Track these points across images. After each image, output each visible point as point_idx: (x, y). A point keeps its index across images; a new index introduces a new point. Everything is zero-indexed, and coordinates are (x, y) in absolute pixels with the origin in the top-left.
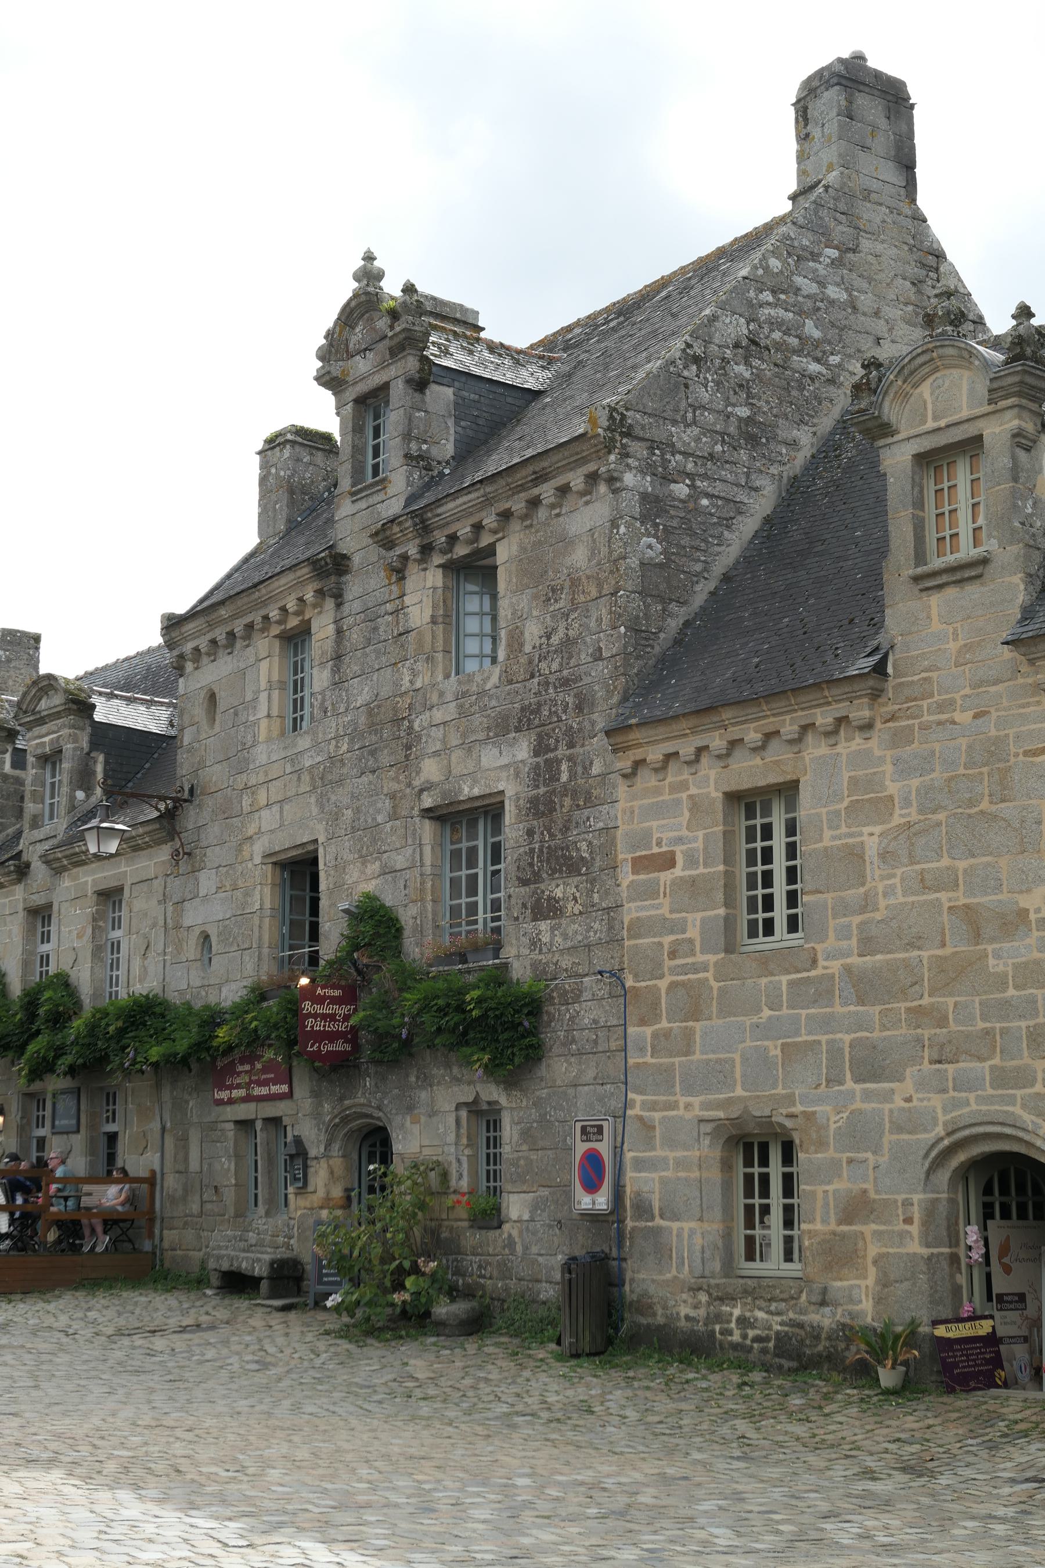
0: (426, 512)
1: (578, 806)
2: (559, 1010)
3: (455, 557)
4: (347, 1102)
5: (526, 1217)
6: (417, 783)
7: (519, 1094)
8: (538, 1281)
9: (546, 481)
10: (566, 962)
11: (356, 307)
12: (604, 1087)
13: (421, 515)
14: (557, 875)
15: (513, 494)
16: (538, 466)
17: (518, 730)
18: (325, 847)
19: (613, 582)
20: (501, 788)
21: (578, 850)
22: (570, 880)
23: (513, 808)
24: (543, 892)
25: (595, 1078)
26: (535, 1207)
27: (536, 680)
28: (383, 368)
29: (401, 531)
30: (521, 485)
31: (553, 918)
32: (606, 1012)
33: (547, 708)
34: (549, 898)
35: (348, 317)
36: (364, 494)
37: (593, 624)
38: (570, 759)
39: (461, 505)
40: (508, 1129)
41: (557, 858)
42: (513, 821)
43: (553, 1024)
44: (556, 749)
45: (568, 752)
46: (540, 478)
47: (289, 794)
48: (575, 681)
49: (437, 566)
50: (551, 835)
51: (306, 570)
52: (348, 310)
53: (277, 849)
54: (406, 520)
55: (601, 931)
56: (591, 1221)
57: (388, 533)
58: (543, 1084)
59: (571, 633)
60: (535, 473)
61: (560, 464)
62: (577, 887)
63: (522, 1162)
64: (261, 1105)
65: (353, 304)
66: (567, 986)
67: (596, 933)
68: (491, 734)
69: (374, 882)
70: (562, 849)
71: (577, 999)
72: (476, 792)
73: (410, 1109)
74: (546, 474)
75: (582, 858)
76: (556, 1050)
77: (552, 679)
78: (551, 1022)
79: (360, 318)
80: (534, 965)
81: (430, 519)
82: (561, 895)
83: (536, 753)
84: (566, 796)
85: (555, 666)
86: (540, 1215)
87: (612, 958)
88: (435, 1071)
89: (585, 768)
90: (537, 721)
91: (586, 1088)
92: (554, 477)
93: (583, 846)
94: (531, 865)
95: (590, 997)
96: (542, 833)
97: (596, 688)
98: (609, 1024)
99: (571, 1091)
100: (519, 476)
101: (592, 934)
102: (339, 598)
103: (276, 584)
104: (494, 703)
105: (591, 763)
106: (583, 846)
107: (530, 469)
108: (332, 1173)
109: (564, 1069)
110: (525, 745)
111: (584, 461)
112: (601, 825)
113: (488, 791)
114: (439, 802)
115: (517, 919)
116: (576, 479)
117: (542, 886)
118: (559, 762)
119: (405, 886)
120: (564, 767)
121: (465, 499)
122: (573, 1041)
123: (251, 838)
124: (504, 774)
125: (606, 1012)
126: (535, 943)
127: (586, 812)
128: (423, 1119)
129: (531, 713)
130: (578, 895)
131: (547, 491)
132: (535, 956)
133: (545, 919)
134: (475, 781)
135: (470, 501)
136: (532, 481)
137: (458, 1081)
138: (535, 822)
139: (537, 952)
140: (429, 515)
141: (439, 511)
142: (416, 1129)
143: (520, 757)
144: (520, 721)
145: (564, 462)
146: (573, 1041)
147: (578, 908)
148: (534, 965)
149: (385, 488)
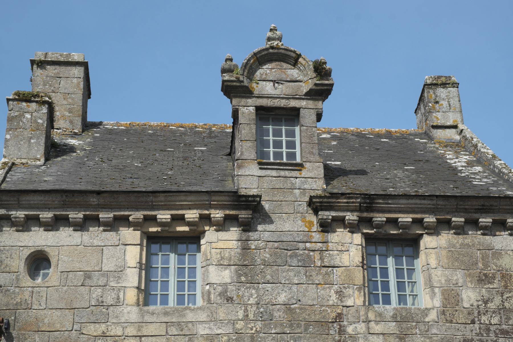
3: (383, 232)
15: (456, 211)
30: (465, 209)
36: (276, 167)
49: (363, 234)
51: (227, 198)
59: (507, 304)
60: (483, 205)
61: (505, 207)
85: (495, 320)
100: (469, 203)
135: (420, 204)
136: (475, 209)
145: (509, 207)
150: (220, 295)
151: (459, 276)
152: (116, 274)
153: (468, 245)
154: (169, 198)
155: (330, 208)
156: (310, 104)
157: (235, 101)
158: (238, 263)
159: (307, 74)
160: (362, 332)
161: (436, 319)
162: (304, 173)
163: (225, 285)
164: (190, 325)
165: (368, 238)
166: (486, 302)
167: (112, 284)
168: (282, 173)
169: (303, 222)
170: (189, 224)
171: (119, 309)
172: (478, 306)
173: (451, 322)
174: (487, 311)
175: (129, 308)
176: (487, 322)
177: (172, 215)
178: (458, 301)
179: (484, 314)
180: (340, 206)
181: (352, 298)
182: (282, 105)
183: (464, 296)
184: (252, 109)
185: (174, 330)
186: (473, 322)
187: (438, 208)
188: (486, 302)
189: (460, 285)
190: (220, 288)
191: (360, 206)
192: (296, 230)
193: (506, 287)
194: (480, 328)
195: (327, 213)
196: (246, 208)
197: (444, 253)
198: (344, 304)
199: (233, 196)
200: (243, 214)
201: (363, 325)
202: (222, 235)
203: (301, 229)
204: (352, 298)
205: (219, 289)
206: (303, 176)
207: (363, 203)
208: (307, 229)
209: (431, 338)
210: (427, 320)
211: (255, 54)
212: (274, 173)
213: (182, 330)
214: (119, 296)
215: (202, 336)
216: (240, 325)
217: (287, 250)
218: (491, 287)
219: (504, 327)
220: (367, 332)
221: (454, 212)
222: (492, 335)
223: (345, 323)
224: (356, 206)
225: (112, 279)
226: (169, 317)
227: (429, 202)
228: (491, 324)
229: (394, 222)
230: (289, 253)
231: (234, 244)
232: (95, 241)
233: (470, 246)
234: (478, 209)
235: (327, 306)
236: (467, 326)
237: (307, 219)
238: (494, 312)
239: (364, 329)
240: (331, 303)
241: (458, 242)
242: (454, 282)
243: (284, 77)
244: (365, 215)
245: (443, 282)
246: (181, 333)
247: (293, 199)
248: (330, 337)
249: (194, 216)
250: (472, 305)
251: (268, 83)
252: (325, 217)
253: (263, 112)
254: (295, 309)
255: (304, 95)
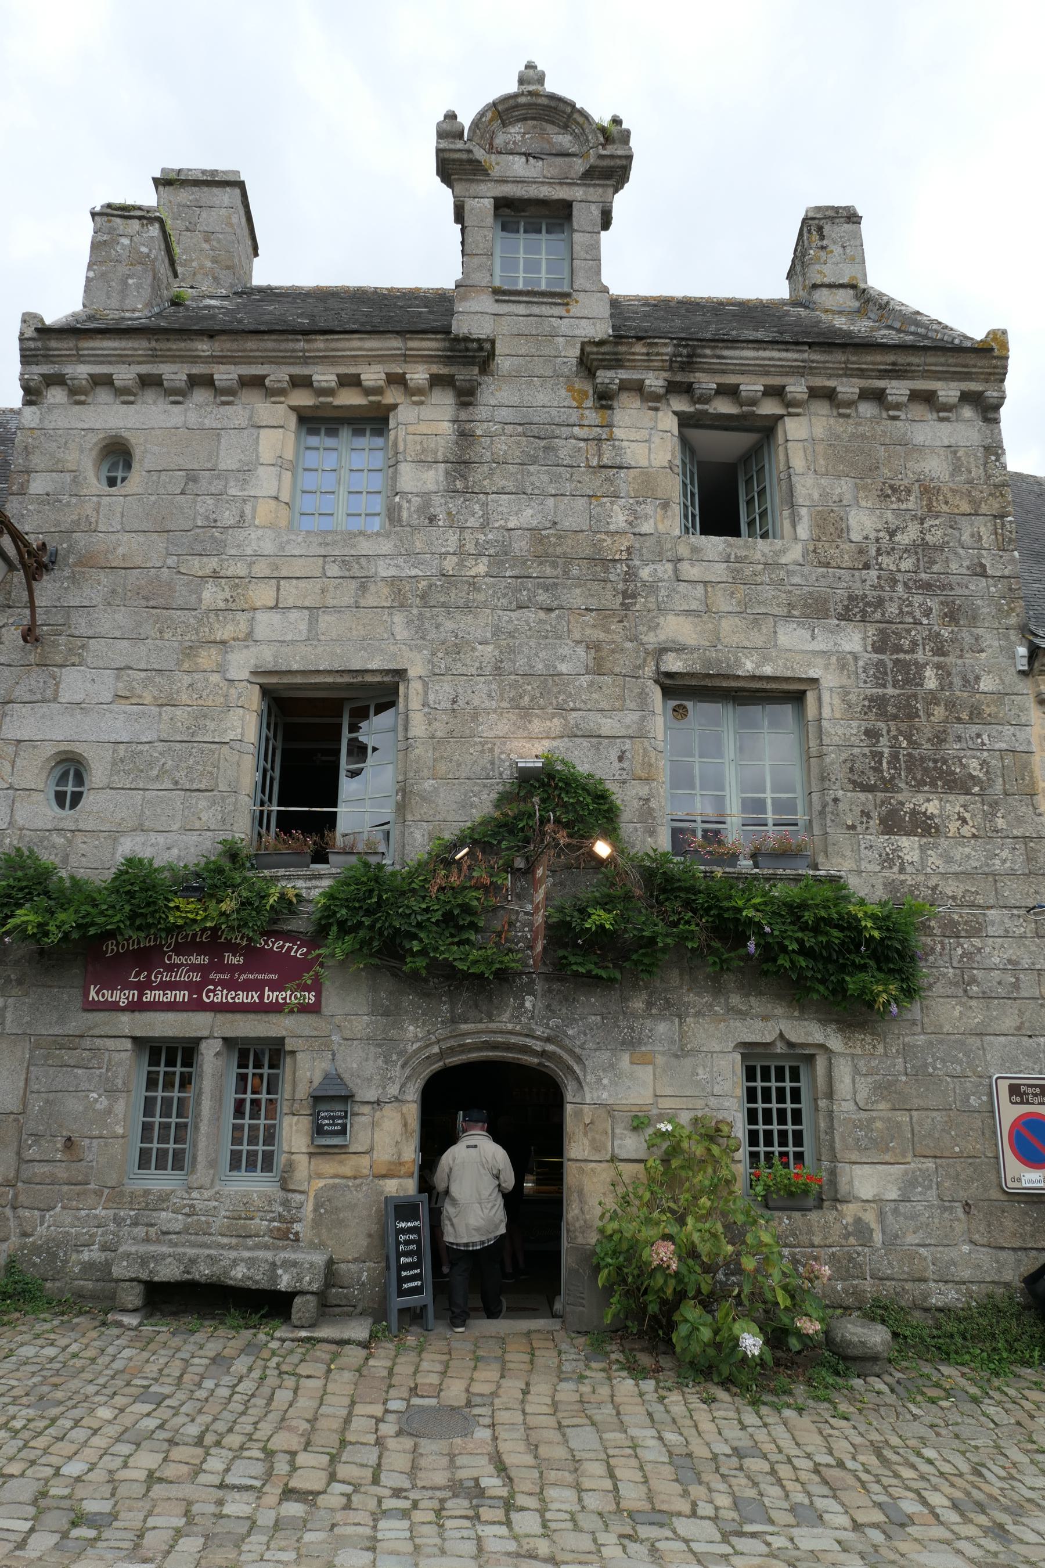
0: (704, 347)
1: (959, 720)
2: (942, 943)
3: (711, 411)
4: (464, 1027)
5: (893, 1194)
6: (652, 640)
7: (869, 1038)
8: (925, 1280)
9: (905, 378)
10: (951, 888)
11: (524, 105)
12: (1035, 1039)
13: (694, 347)
14: (926, 788)
15: (846, 375)
16: (902, 359)
17: (841, 617)
18: (425, 685)
19: (997, 506)
20: (812, 674)
21: (964, 766)
22: (951, 797)
23: (836, 701)
24: (902, 804)
25: (1018, 1028)
26: (909, 1183)
27: (873, 573)
28: (561, 184)
29: (648, 354)
31: (922, 836)
32: (1031, 953)
33: (895, 605)
34: (914, 812)
35: (507, 110)
37: (966, 537)
38: (938, 666)
39: (764, 359)
40: (848, 1080)
41: (926, 770)
42: (838, 715)
43: (931, 958)
44: (912, 651)
45: (936, 659)
46: (896, 373)
47: (331, 602)
48: (943, 587)
49: (675, 413)
50: (911, 742)
52: (511, 102)
53: (295, 667)
54: (665, 344)
55: (1013, 862)
56: (1025, 1203)
57: (622, 349)
58: (919, 1029)
59: (928, 537)
60: (894, 364)
61: (933, 368)
62: (964, 806)
63: (879, 1124)
64: (220, 1017)
65: (522, 100)
66: (956, 917)
67: (1004, 861)
68: (795, 613)
69: (546, 743)
70: (935, 761)
71: (976, 930)
72: (768, 670)
73: (630, 1044)
74: (906, 371)
75: (973, 777)
76: (938, 989)
77: (899, 577)
78: (927, 955)
79: (518, 121)
80: (891, 886)
81: (705, 356)
82: (936, 812)
83: (877, 649)
84: (937, 704)
85: (906, 565)
86: (921, 1193)
87: (1036, 892)
88: (691, 998)
89: (966, 681)
90: (878, 616)
91: (1002, 1039)
92: (912, 378)
93: (974, 764)
94: (877, 769)
95: (1001, 933)
96: (896, 738)
97: (979, 602)
98: (1038, 967)
99: (974, 1041)
100: (869, 358)
101: (997, 862)
102: (466, 396)
103: (356, 344)
104: (796, 580)
105: (978, 678)
106: (974, 764)
107: (891, 358)
108: (405, 1125)
109: (957, 1013)
110: (857, 637)
111: (967, 377)
112: (1004, 746)
113: (789, 674)
114: (698, 668)
115: (853, 827)
116: (948, 392)
117: (900, 797)
118: (921, 667)
119: (621, 759)
120: (929, 672)
121: (776, 354)
122: (973, 980)
123: (223, 642)
124: (820, 661)
125: (1031, 953)
126: (888, 860)
127: (975, 729)
128: (660, 1060)
129: (868, 604)
130: (967, 815)
131: (898, 389)
132: (893, 873)
133: (908, 835)
134: (765, 659)
135: (780, 359)
136: (880, 371)
137: (742, 1015)
138: (881, 725)
139: (896, 869)
140: (708, 352)
141: (726, 353)
142: (645, 1073)
143: (847, 647)
144: (847, 608)
145: (940, 368)
146: (973, 980)
147: (966, 831)
148: (891, 886)
149: (567, 304)
150: (417, 511)
151: (844, 488)
152: (240, 476)
153: (863, 436)
154: (333, 345)
155: (616, 363)
156: (594, 193)
157: (458, 187)
158: (452, 459)
159: (587, 140)
160: (666, 577)
161: (801, 561)
162: (574, 310)
163: (425, 495)
164: (363, 561)
165: (685, 421)
166: (892, 534)
167: (232, 491)
168: (535, 310)
169: (569, 391)
170: (368, 392)
171: (241, 534)
172: (877, 540)
173: (827, 565)
174: (893, 549)
175: (260, 532)
176: (893, 568)
177: (338, 375)
178: (842, 532)
179: (888, 554)
180: (634, 360)
181: (652, 521)
182: (541, 196)
183: (853, 522)
184: (488, 204)
185: (336, 568)
186: (867, 566)
187: (811, 368)
188: (892, 534)
189: (845, 502)
190: (419, 499)
191: (671, 361)
192: (556, 404)
193: (930, 507)
194: (879, 577)
195: (610, 374)
196: (467, 360)
197: (820, 448)
198: (637, 530)
199: (444, 340)
200: (464, 374)
201: (669, 566)
202: (426, 412)
203: (566, 404)
204: (652, 521)
205: (416, 501)
206: (571, 314)
207: (675, 356)
208: (575, 404)
209: (790, 592)
210: (783, 561)
211: (494, 104)
212: (521, 309)
213: (349, 570)
214: (243, 512)
215: (384, 579)
216: (450, 564)
217: (539, 438)
218: (904, 506)
219: (923, 576)
220: (673, 578)
221: (840, 376)
222: (900, 588)
223: (637, 563)
224: (663, 361)
225: (232, 483)
226: (329, 548)
227: (795, 356)
228: (899, 571)
229: (731, 392)
230: (543, 443)
231: (446, 428)
232: (207, 421)
233: (867, 438)
234: (886, 371)
235: (606, 533)
236: (857, 573)
237: (577, 386)
238: (906, 551)
239: (670, 572)
240: (612, 528)
241: (845, 431)
242: (836, 498)
243: (546, 147)
244: (679, 378)
245: (816, 496)
246: (347, 574)
247: (554, 353)
248: (609, 585)
249: (375, 377)
250: (866, 538)
251: (517, 158)
252: (607, 381)
253: (507, 211)
254: (548, 537)
255: (581, 178)
